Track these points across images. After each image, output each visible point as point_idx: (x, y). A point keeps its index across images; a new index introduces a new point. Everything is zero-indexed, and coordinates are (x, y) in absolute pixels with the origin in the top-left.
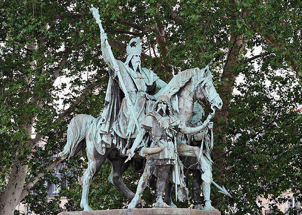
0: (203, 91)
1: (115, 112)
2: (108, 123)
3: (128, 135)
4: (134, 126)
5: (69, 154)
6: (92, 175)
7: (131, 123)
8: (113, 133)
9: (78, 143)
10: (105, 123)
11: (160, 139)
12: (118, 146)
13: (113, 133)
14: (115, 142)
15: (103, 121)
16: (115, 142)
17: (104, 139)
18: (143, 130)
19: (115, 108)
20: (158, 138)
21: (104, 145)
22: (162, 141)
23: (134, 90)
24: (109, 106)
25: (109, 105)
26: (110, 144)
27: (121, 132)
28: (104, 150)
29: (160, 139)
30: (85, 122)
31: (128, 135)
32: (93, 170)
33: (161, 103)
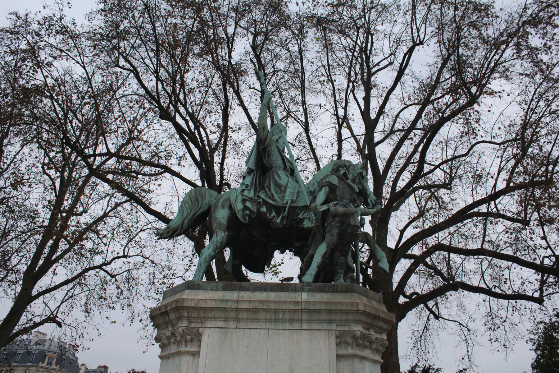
0: (362, 181)
1: (258, 183)
2: (253, 190)
3: (287, 203)
4: (296, 194)
5: (177, 230)
6: (217, 251)
7: (288, 191)
8: (261, 200)
9: (197, 214)
10: (249, 190)
11: (349, 202)
12: (268, 215)
13: (261, 200)
14: (264, 209)
15: (246, 187)
16: (264, 209)
17: (248, 204)
18: (327, 188)
19: (258, 180)
20: (345, 201)
21: (248, 212)
22: (351, 204)
23: (282, 166)
24: (252, 175)
25: (252, 175)
26: (255, 210)
27: (274, 200)
28: (247, 218)
29: (349, 202)
30: (209, 195)
31: (287, 203)
32: (221, 243)
33: (343, 167)
